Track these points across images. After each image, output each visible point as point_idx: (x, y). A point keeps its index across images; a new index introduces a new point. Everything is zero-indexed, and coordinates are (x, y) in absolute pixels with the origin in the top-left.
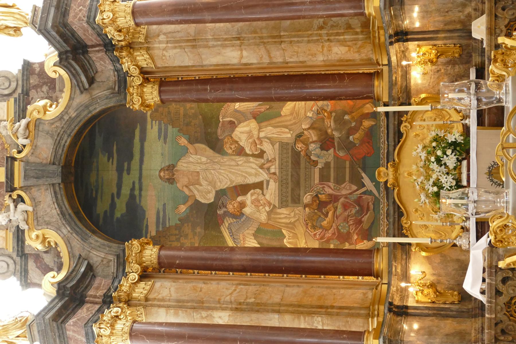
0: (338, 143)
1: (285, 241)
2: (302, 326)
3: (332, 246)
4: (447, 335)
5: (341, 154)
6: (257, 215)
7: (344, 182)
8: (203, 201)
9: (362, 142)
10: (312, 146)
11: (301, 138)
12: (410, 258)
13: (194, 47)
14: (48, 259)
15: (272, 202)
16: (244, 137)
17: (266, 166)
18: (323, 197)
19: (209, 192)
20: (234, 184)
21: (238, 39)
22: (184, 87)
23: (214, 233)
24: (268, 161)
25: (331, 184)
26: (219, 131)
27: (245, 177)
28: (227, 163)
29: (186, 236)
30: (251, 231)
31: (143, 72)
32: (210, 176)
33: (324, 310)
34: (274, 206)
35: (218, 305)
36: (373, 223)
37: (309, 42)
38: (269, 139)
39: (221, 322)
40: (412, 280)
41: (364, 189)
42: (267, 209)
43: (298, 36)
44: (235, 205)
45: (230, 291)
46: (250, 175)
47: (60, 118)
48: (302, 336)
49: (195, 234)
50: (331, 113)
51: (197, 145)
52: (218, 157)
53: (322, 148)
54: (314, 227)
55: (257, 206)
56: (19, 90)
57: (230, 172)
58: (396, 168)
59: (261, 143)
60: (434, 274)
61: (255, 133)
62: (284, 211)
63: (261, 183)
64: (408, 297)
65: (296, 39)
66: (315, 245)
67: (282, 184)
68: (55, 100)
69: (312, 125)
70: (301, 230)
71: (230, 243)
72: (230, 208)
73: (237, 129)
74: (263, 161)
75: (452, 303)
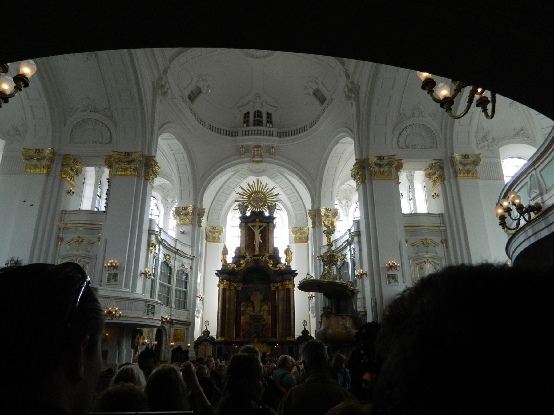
14: (238, 263)
16: (265, 307)
31: (277, 287)
47: (269, 267)
56: (275, 256)
62: (248, 317)
68: (273, 265)
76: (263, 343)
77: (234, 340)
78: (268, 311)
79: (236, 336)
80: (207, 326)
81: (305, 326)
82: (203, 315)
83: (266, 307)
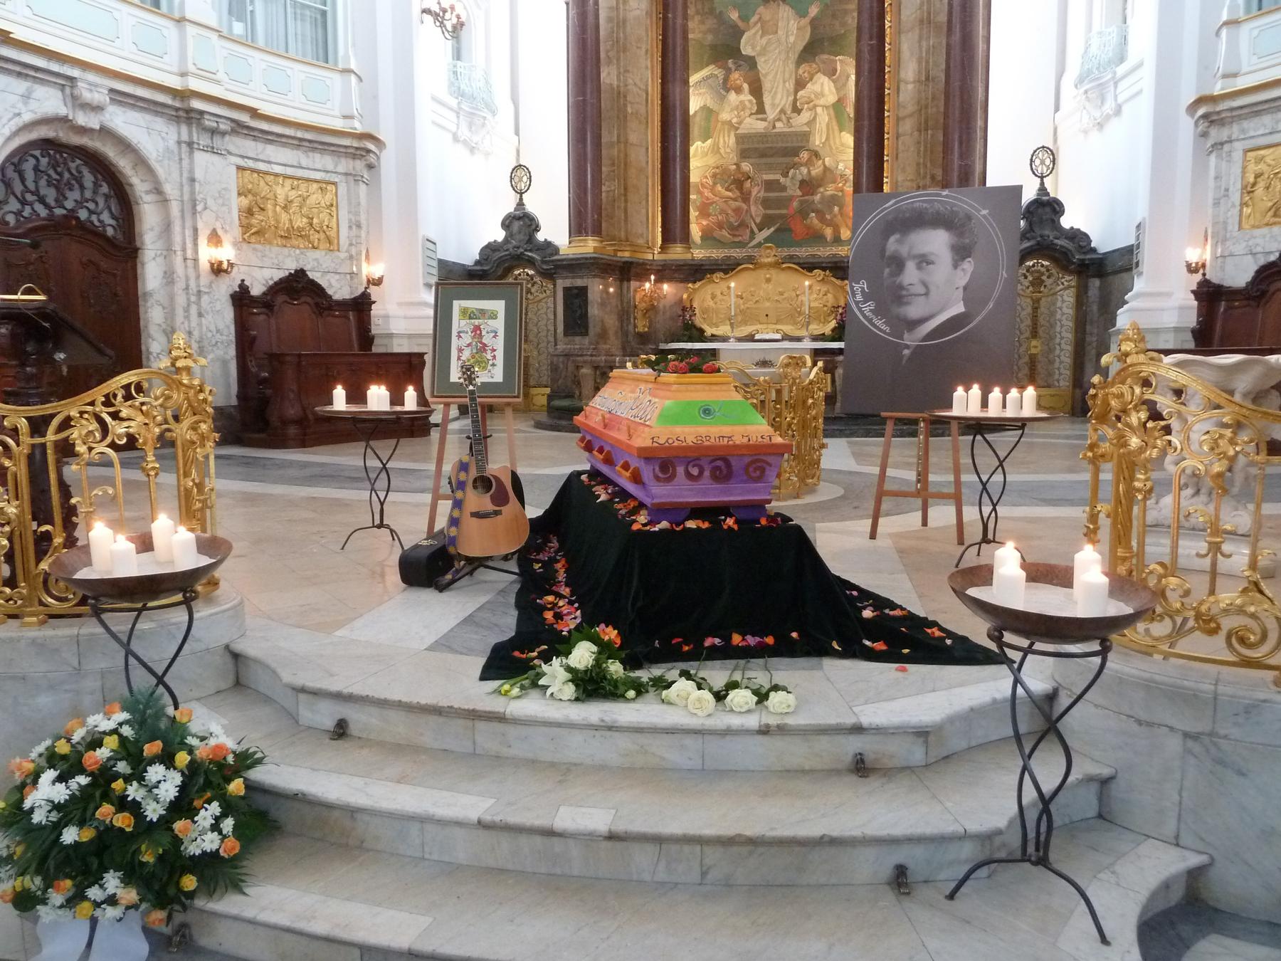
0: (807, 201)
1: (699, 143)
2: (604, 169)
3: (692, 197)
4: (602, 321)
5: (795, 204)
6: (727, 109)
7: (765, 209)
8: (743, 41)
9: (809, 227)
10: (804, 170)
11: (814, 157)
12: (682, 281)
13: (921, 21)
15: (742, 126)
17: (783, 117)
18: (747, 184)
19: (753, 48)
20: (762, 78)
21: (927, 79)
22: (875, 10)
23: (706, 58)
24: (789, 119)
25: (762, 194)
26: (825, 57)
27: (770, 92)
28: (787, 69)
29: (702, 22)
30: (710, 103)
32: (772, 48)
33: (622, 191)
34: (737, 129)
35: (622, 70)
36: (720, 241)
37: (918, 164)
38: (815, 118)
39: (603, 75)
40: (659, 285)
41: (756, 230)
42: (734, 120)
43: (925, 151)
44: (738, 82)
45: (638, 83)
46: (773, 98)
48: (593, 170)
49: (705, 33)
50: (842, 191)
51: (809, 29)
52: (794, 56)
53: (802, 182)
54: (714, 176)
55: (737, 108)
57: (776, 73)
58: (777, 265)
59: (810, 110)
60: (664, 307)
61: (822, 102)
62: (732, 140)
63: (765, 113)
64: (640, 281)
65: (922, 149)
66: (694, 178)
67: (762, 137)
69: (829, 169)
70: (712, 160)
71: (694, 79)
72: (736, 76)
73: (826, 79)
74: (789, 112)
75: (635, 326)
76: (809, 267)
77: (655, 255)
78: (838, 106)
79: (668, 238)
80: (521, 194)
81: (1042, 178)
82: (518, 152)
83: (824, 89)
